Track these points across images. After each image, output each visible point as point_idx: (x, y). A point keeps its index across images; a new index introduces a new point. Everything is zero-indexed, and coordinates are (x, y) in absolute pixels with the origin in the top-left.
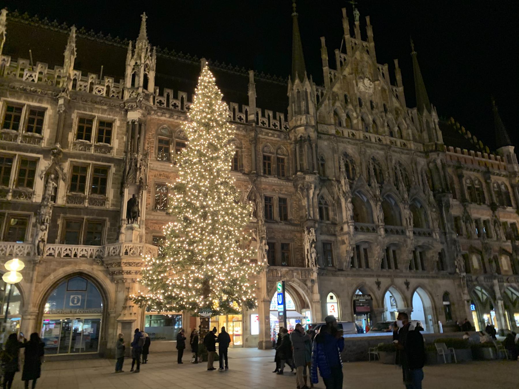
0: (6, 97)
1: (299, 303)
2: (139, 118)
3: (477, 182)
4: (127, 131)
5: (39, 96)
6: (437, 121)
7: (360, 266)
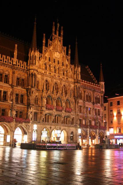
1: (23, 132)
3: (90, 94)
6: (80, 71)
7: (46, 121)
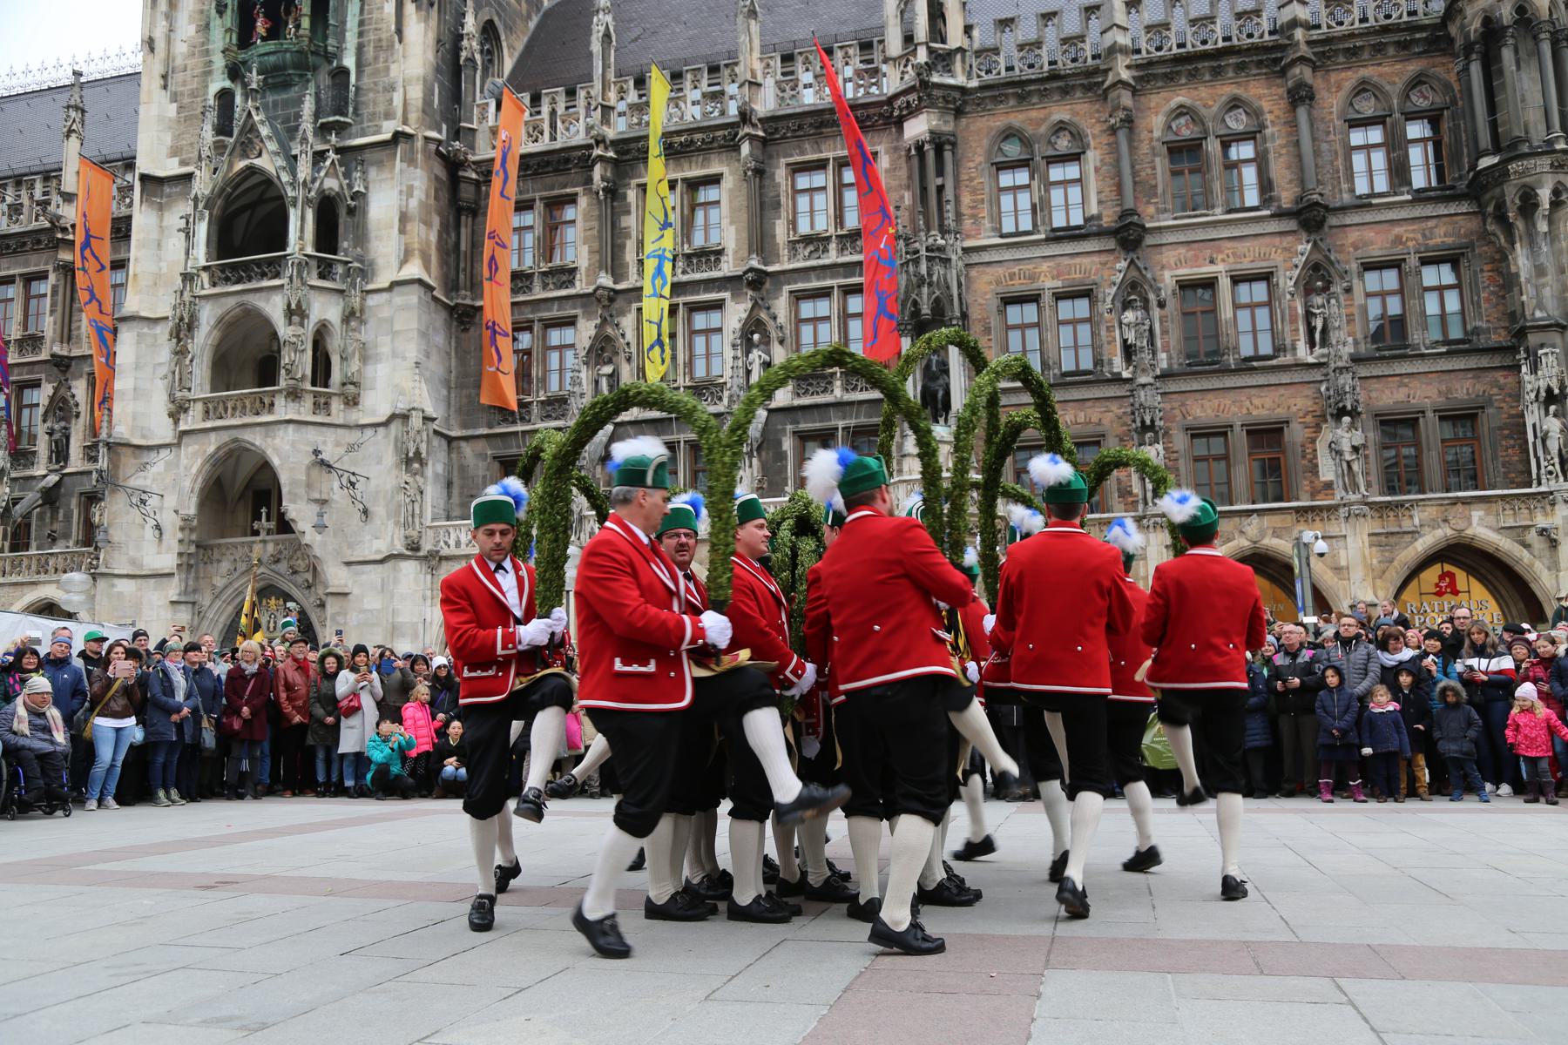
0: (640, 176)
2: (931, 132)
4: (910, 177)
5: (699, 150)
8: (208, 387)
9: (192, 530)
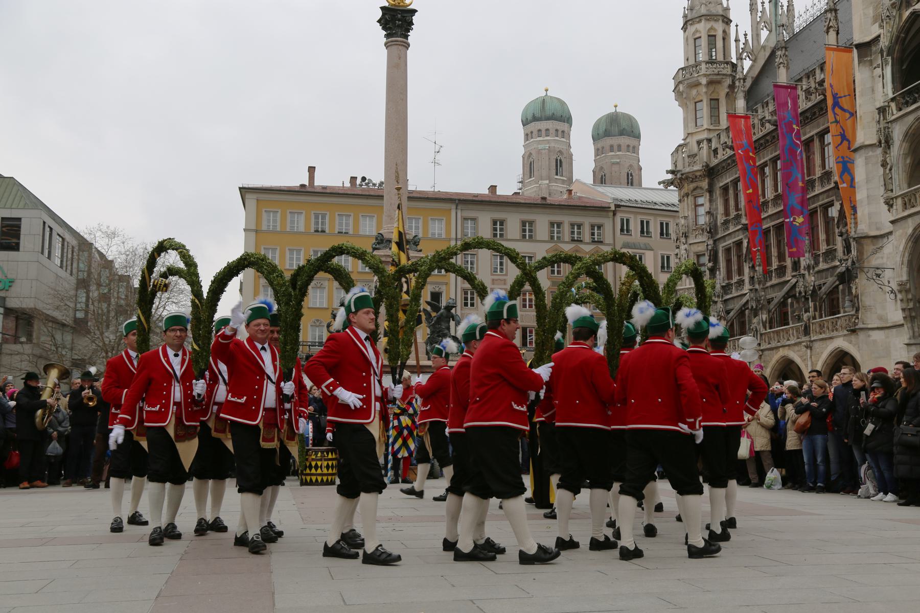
8: (905, 185)
9: (907, 291)
